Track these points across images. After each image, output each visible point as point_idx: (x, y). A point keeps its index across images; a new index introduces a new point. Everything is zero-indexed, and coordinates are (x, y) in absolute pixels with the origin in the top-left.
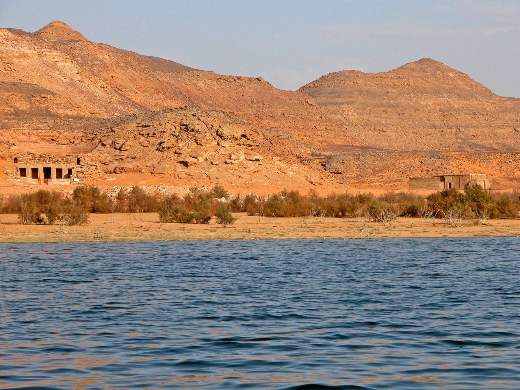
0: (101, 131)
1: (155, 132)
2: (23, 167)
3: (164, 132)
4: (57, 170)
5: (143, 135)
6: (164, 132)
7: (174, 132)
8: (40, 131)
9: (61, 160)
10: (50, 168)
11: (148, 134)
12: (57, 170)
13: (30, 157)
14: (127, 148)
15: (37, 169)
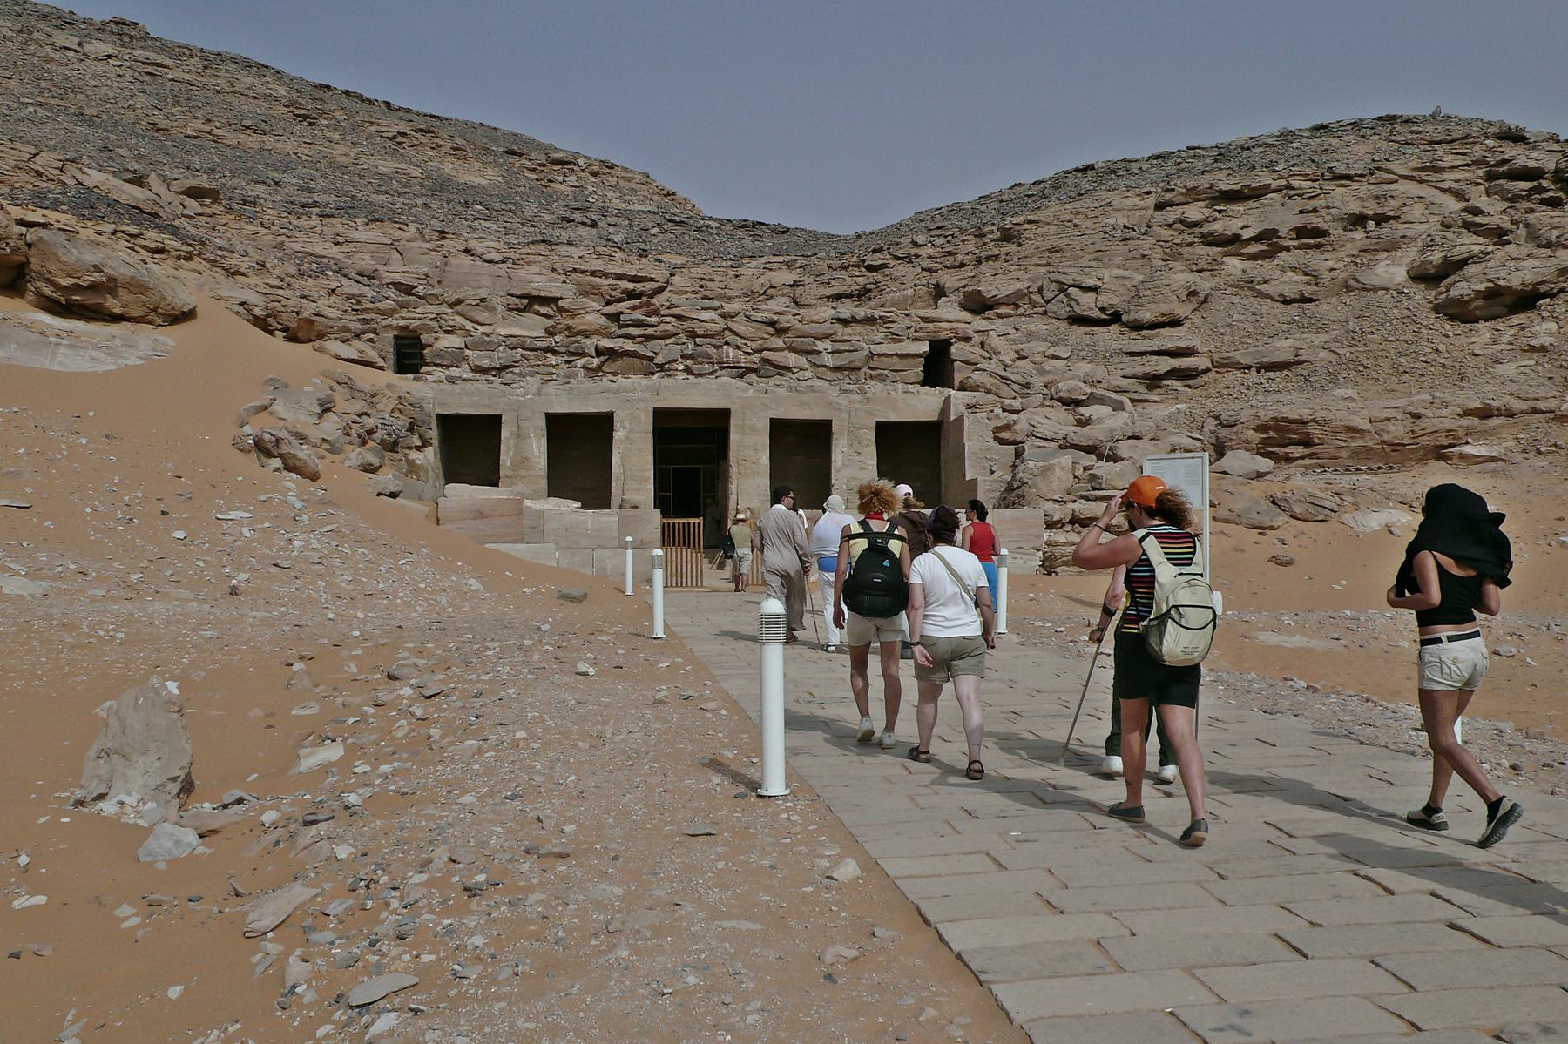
0: (913, 251)
1: (1315, 221)
2: (472, 399)
3: (1381, 219)
4: (781, 430)
5: (1231, 242)
6: (1381, 219)
7: (1477, 212)
8: (563, 250)
9: (792, 359)
10: (723, 415)
11: (1267, 236)
12: (781, 430)
13: (531, 327)
14: (1182, 310)
15: (602, 425)
